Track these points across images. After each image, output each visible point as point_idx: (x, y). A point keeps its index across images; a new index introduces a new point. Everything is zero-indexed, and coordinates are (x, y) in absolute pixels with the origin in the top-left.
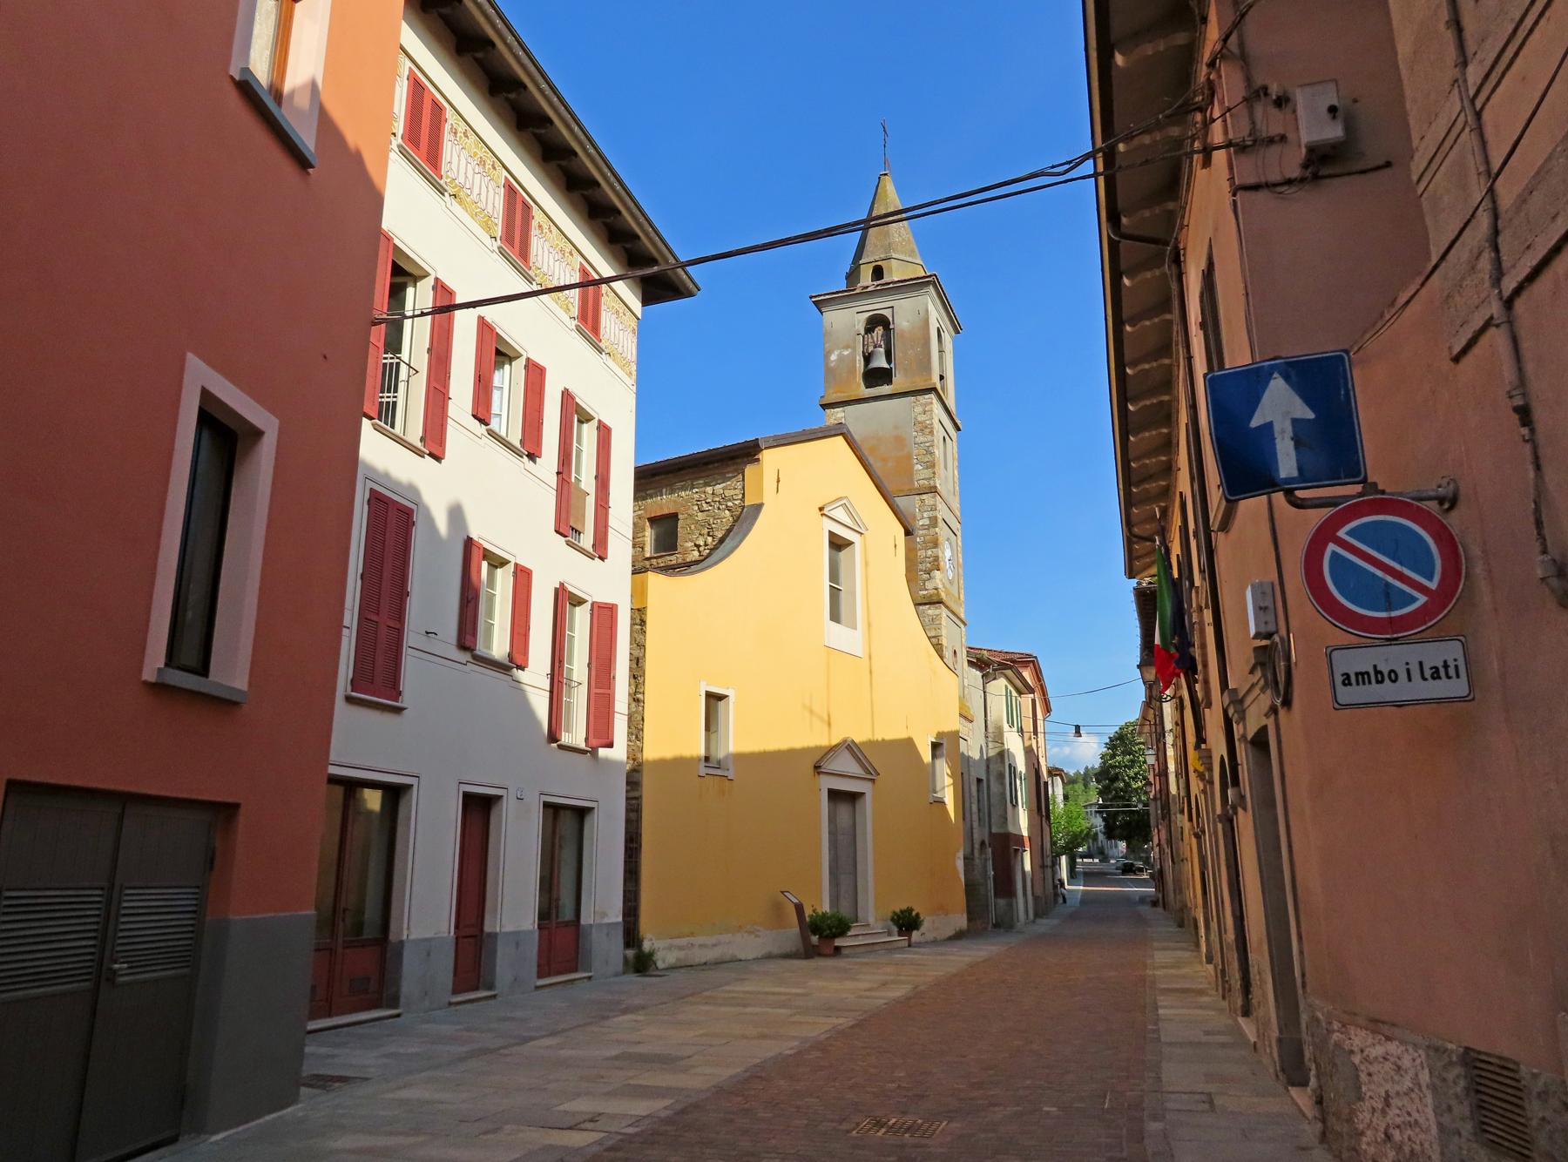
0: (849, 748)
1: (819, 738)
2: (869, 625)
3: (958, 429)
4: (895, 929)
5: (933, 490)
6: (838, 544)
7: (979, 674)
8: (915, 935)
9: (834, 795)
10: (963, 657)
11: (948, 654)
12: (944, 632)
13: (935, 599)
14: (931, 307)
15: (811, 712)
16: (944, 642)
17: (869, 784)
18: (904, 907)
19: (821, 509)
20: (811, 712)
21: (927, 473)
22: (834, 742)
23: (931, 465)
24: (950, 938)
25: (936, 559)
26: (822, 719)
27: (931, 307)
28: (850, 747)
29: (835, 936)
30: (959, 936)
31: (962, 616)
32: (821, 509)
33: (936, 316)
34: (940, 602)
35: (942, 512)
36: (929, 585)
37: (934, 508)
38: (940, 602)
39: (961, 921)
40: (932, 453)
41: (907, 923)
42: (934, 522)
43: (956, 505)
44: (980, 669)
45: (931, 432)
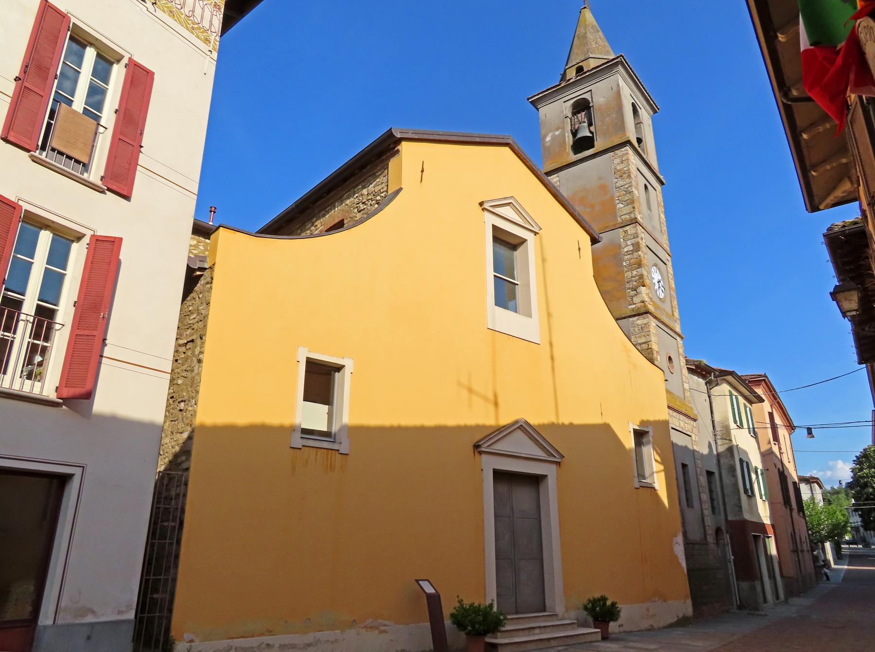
0: (521, 428)
1: (482, 416)
2: (549, 315)
3: (662, 183)
4: (590, 620)
5: (634, 222)
6: (505, 242)
7: (702, 381)
8: (613, 626)
9: (499, 475)
10: (680, 364)
11: (661, 359)
12: (653, 338)
13: (642, 310)
14: (621, 83)
15: (470, 390)
16: (655, 347)
17: (554, 467)
18: (597, 595)
19: (481, 204)
20: (470, 390)
21: (628, 209)
22: (504, 421)
23: (631, 202)
24: (671, 626)
25: (641, 276)
26: (486, 399)
27: (621, 83)
28: (522, 427)
29: (485, 633)
30: (682, 622)
31: (678, 330)
32: (481, 204)
33: (628, 94)
34: (647, 312)
35: (645, 240)
36: (636, 300)
37: (636, 236)
38: (647, 312)
39: (687, 608)
40: (631, 193)
41: (602, 614)
42: (637, 247)
43: (664, 240)
44: (704, 377)
45: (629, 176)
